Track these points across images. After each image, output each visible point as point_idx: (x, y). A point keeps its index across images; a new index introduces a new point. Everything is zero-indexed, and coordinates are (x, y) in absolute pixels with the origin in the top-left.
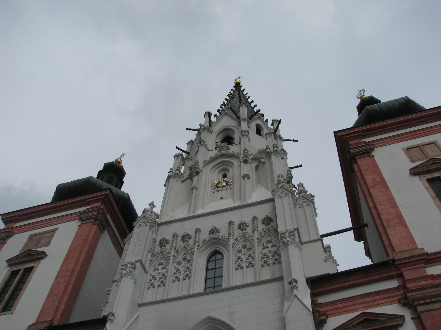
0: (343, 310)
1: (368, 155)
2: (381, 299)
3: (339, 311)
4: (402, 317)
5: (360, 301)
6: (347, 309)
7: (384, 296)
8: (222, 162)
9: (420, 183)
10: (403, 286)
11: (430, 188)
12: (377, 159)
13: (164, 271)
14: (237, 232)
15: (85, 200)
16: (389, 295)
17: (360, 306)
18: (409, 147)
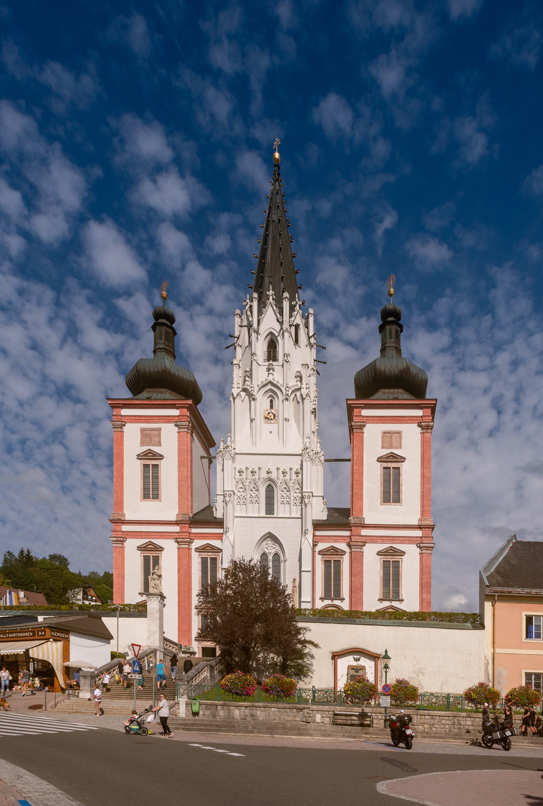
0: (325, 540)
1: (361, 431)
2: (341, 539)
3: (323, 540)
4: (345, 552)
5: (332, 538)
6: (326, 541)
7: (342, 538)
8: (270, 390)
9: (379, 468)
10: (350, 537)
11: (383, 475)
12: (365, 435)
13: (243, 494)
14: (281, 476)
15: (175, 404)
16: (344, 538)
17: (332, 540)
18: (385, 432)
